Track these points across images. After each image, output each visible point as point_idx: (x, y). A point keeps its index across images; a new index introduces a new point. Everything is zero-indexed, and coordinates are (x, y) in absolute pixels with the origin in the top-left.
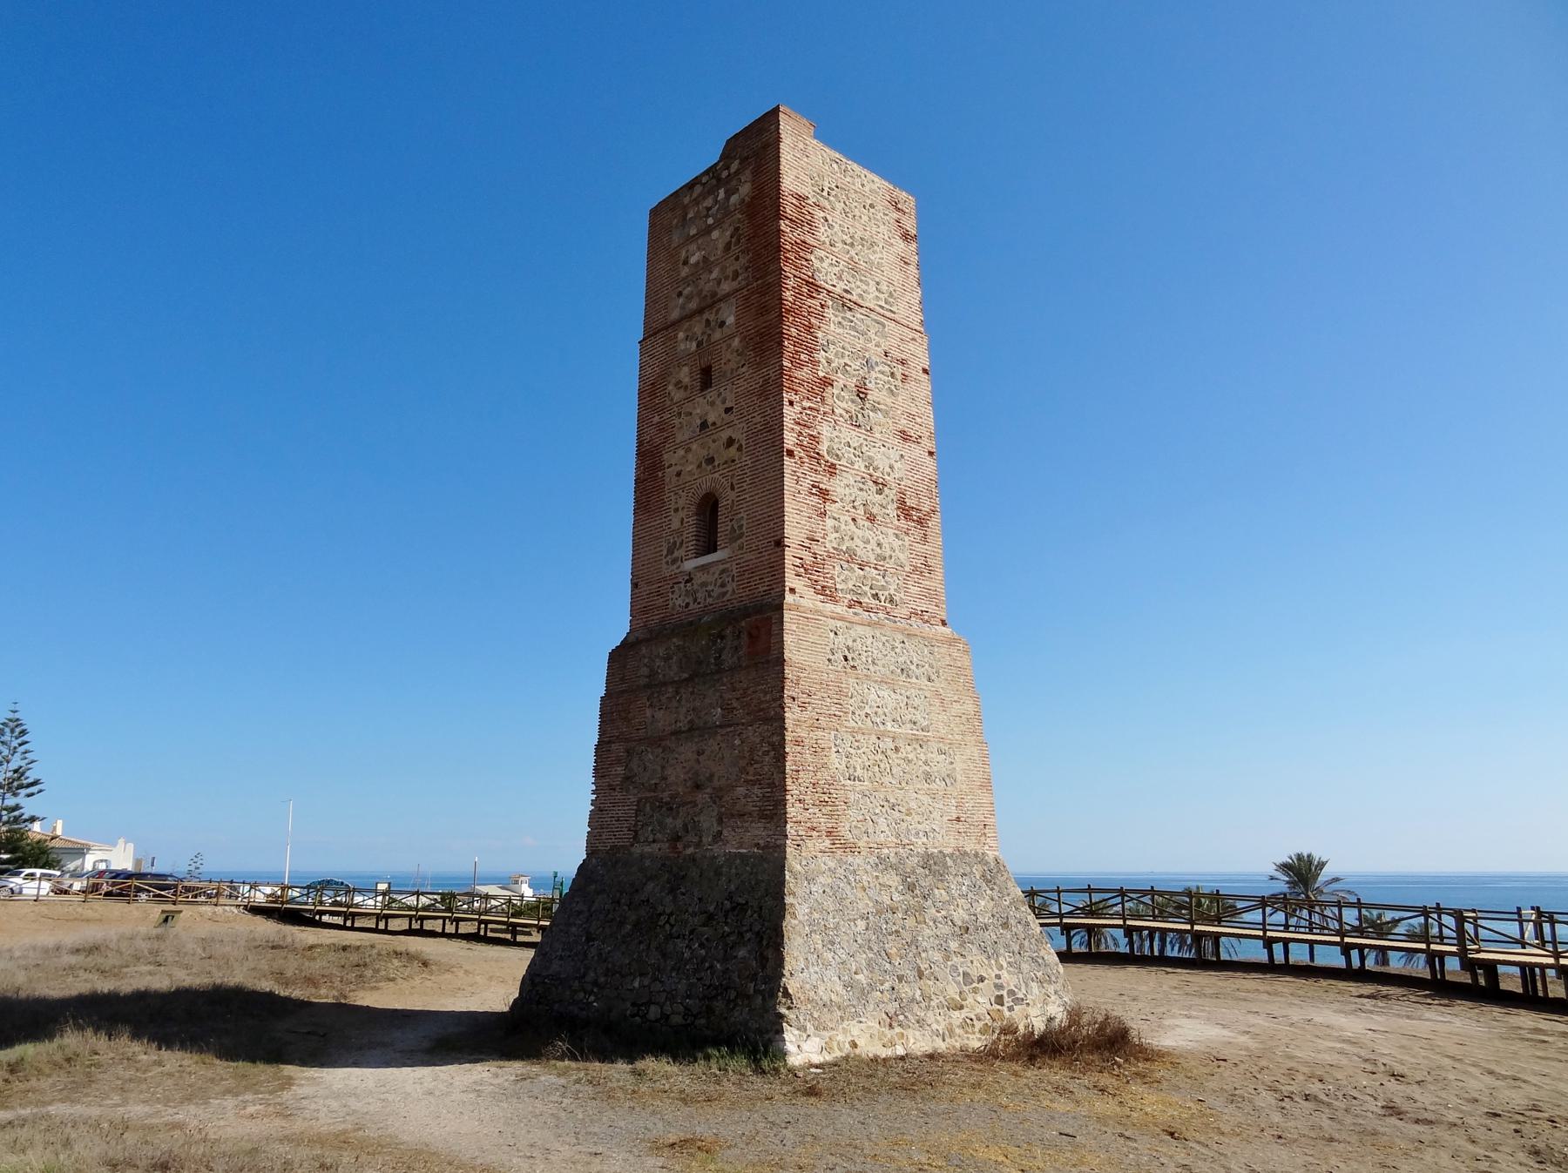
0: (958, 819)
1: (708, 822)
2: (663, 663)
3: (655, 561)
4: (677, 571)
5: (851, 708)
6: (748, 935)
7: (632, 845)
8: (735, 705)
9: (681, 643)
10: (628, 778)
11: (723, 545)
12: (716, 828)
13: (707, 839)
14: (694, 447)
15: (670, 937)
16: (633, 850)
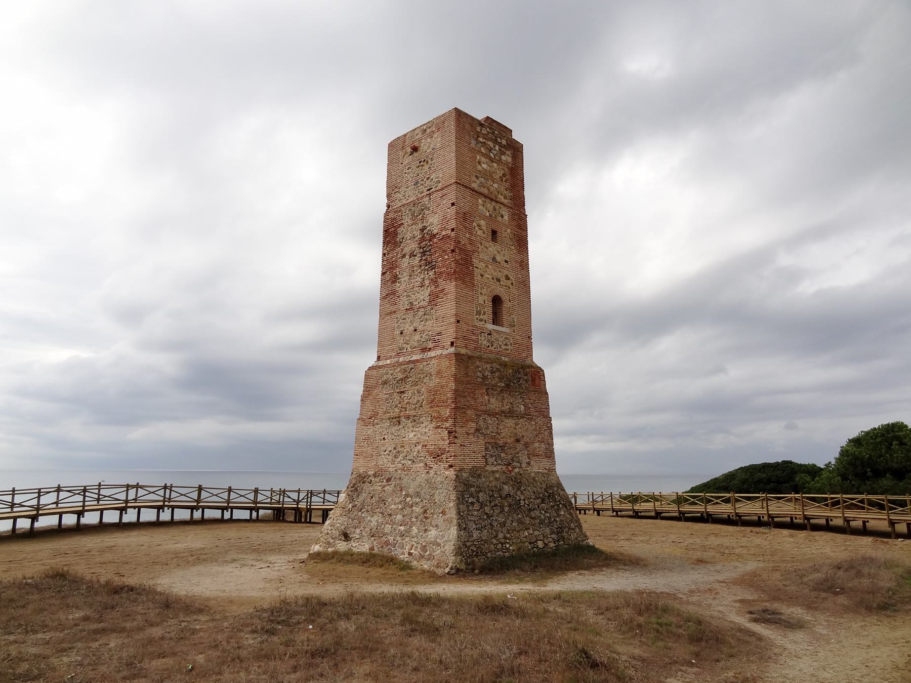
1: (525, 460)
2: (490, 374)
3: (470, 314)
4: (484, 326)
6: (561, 506)
7: (486, 466)
8: (530, 406)
9: (499, 367)
10: (477, 430)
11: (506, 326)
12: (527, 460)
13: (524, 465)
14: (490, 267)
15: (530, 510)
16: (486, 468)
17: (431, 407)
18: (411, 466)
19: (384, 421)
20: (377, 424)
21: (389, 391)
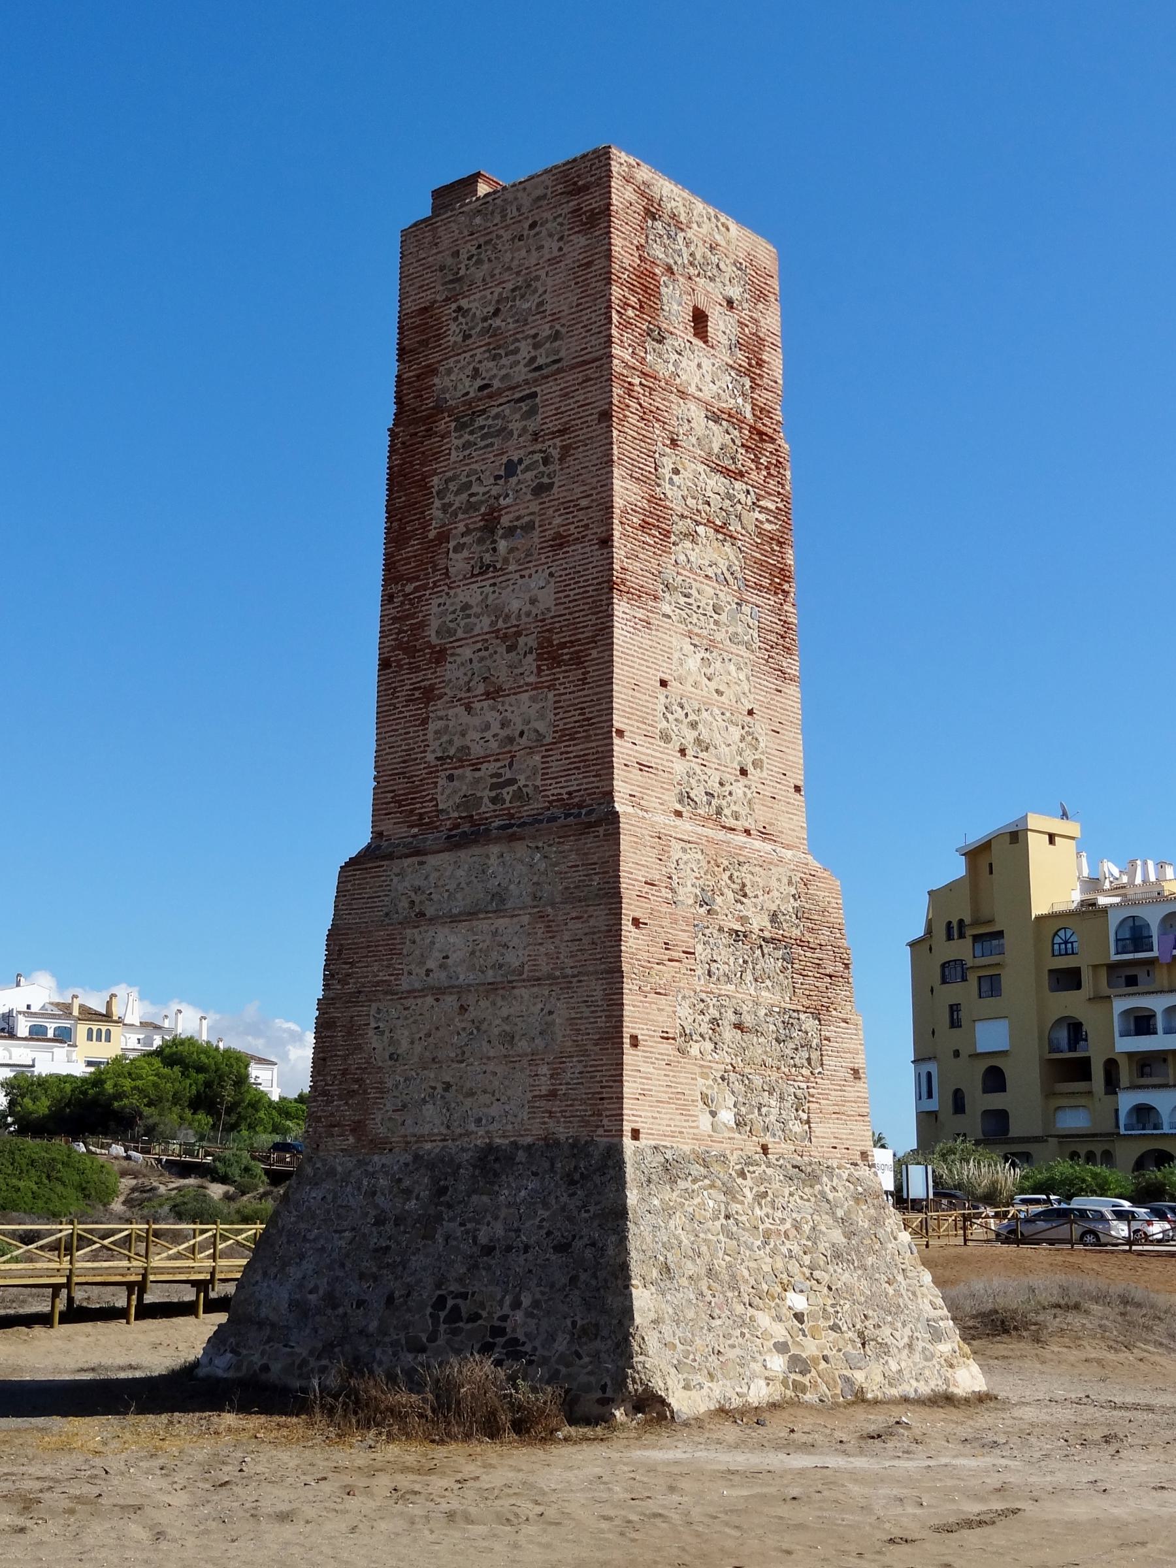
0: (553, 1094)
5: (406, 969)
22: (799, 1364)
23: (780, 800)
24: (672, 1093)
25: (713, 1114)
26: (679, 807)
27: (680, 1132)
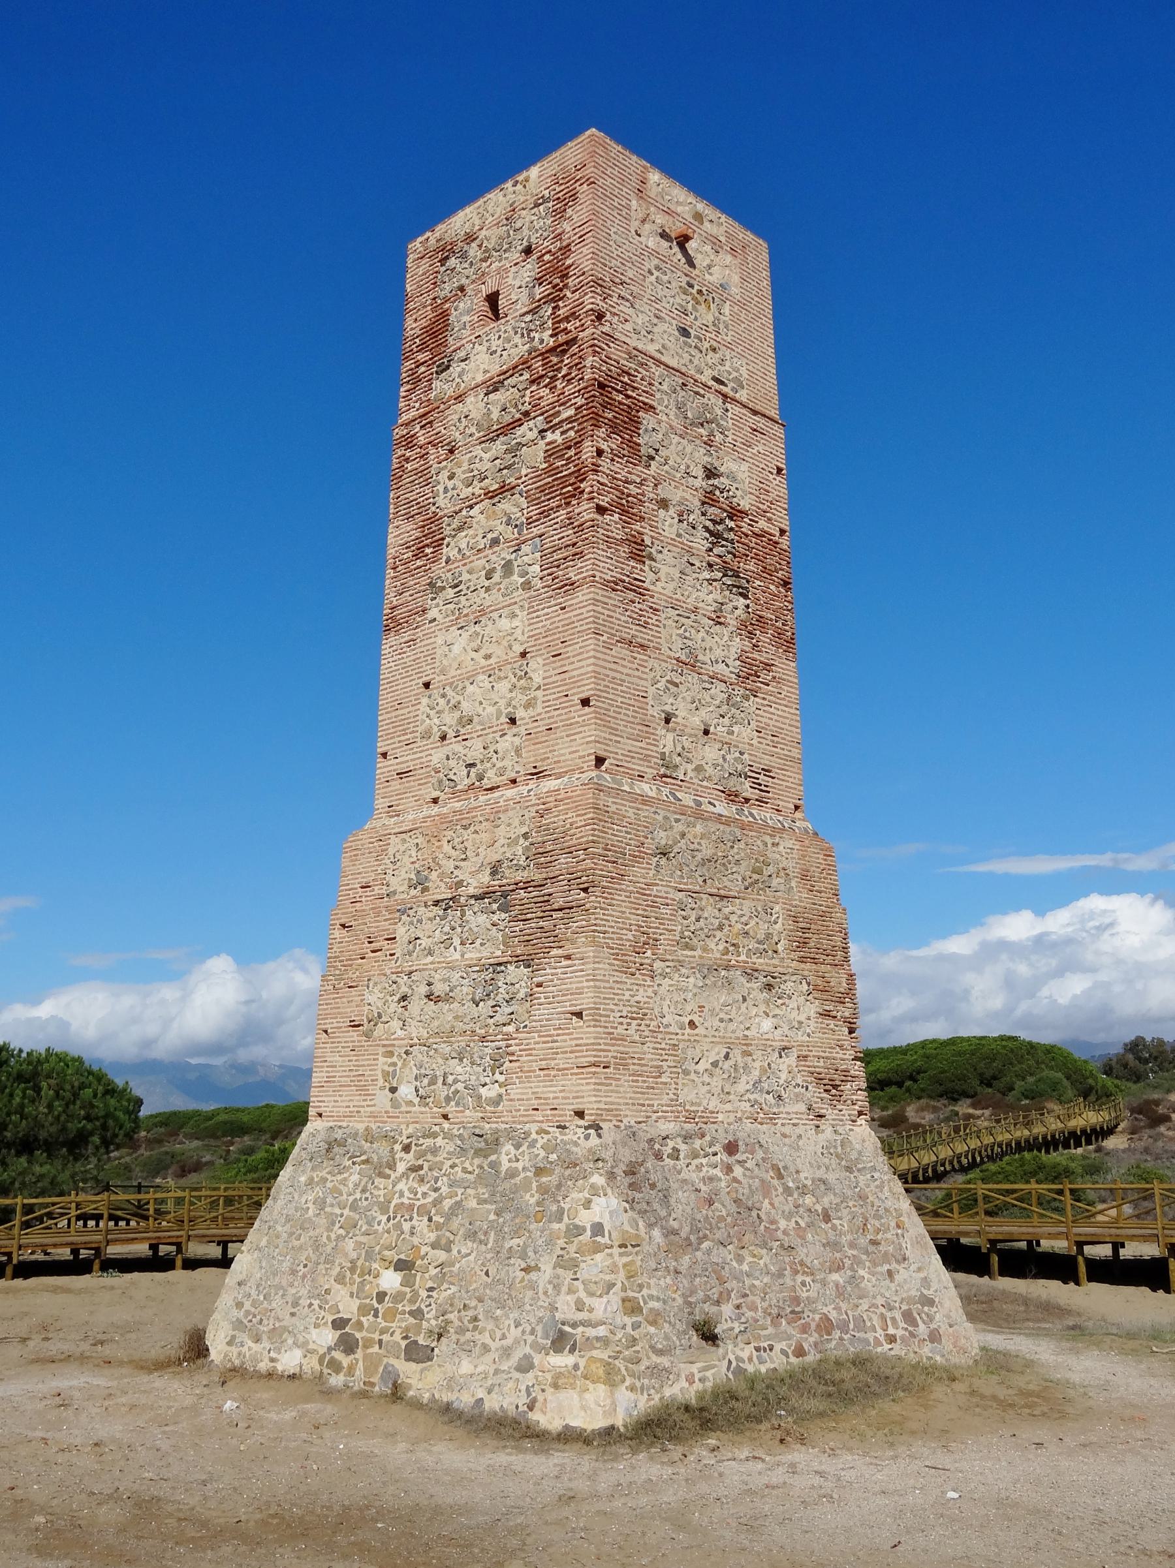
17: (802, 960)
18: (775, 1110)
19: (683, 971)
20: (664, 976)
21: (686, 884)
22: (348, 1345)
23: (556, 728)
24: (354, 1076)
25: (393, 1090)
26: (435, 794)
27: (358, 1112)
